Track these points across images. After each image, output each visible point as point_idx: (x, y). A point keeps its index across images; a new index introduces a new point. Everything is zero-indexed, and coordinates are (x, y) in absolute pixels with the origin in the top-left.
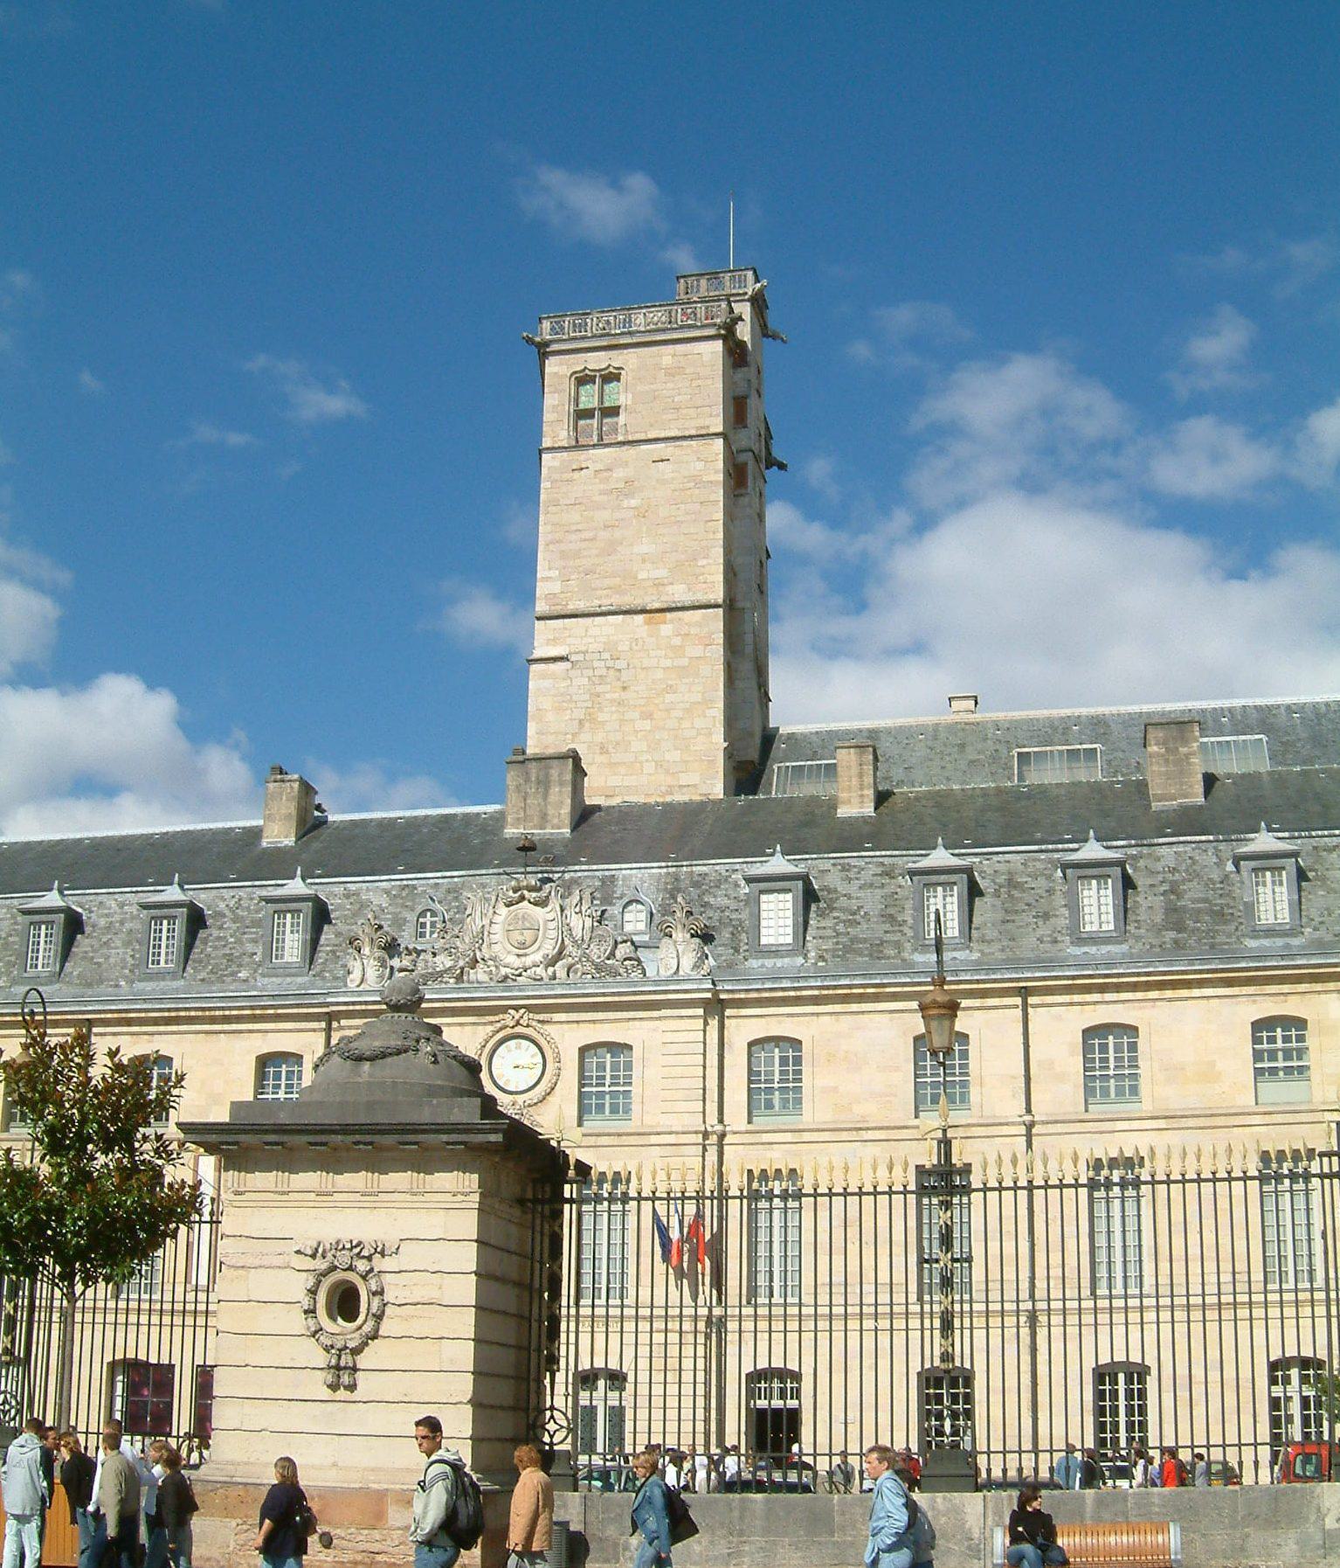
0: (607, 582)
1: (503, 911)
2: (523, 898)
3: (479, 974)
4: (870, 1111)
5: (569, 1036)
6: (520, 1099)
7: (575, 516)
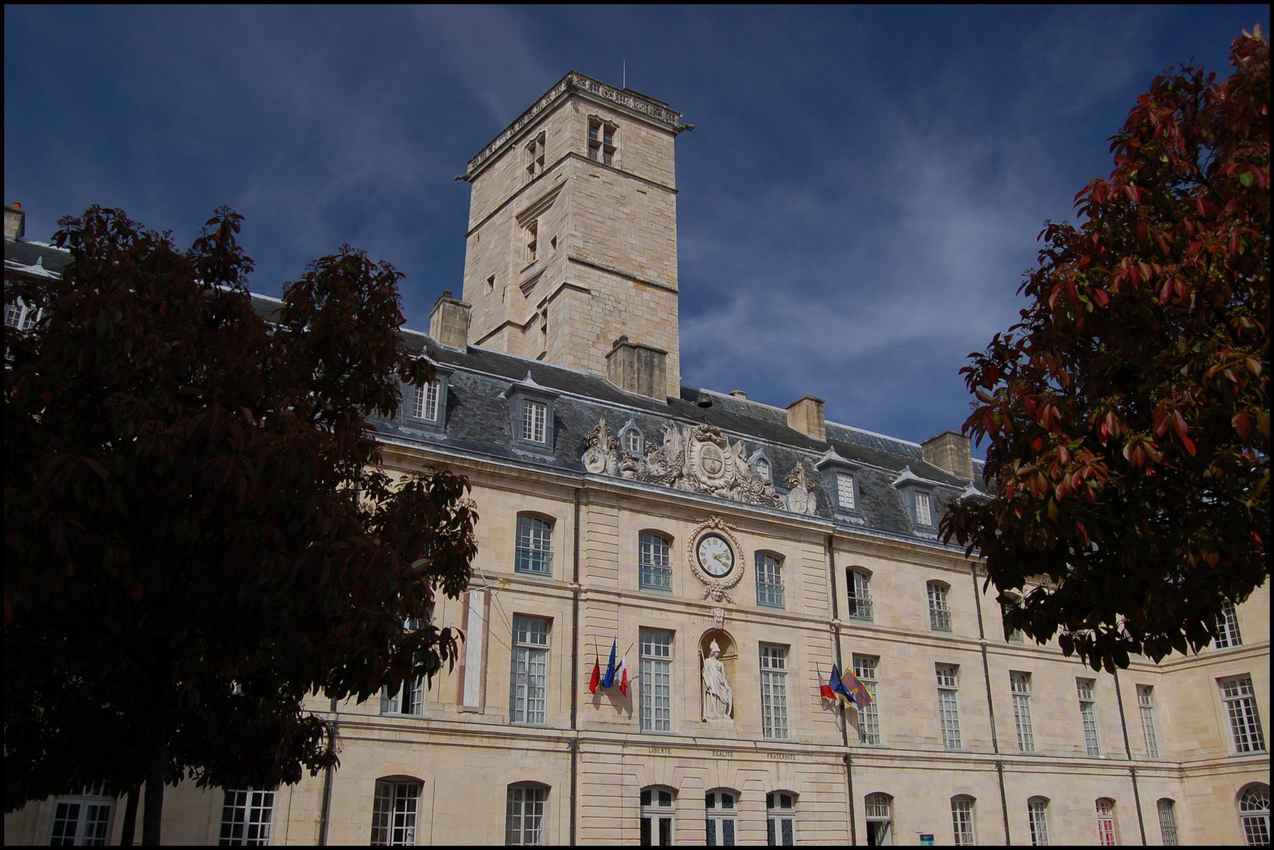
0: (612, 253)
1: (698, 445)
2: (710, 439)
3: (685, 484)
4: (908, 623)
5: (750, 543)
6: (722, 581)
7: (590, 204)
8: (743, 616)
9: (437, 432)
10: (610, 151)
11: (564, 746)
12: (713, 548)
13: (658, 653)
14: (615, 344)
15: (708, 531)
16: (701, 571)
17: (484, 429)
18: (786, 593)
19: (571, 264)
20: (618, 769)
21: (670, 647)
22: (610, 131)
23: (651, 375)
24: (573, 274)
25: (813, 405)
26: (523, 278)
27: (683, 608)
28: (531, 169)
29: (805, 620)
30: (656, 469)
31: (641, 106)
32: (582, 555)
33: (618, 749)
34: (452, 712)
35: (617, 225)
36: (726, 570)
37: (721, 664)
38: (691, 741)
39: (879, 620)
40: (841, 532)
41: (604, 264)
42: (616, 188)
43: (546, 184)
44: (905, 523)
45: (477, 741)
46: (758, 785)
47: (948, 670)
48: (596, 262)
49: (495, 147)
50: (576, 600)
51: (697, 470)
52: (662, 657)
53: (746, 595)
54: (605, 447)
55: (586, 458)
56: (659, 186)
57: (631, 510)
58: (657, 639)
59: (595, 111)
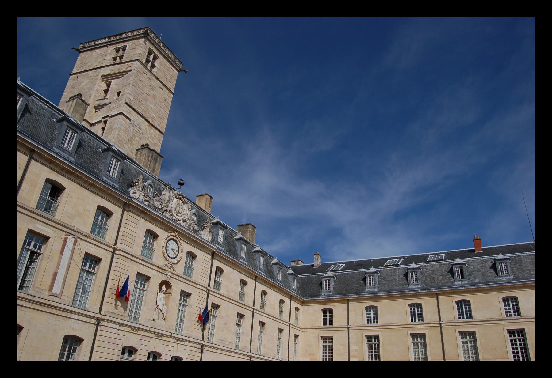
1: (176, 200)
2: (180, 199)
5: (187, 247)
6: (173, 260)
7: (140, 84)
8: (177, 277)
9: (70, 156)
10: (153, 66)
11: (94, 321)
12: (172, 245)
13: (141, 286)
14: (142, 146)
16: (165, 254)
17: (91, 162)
18: (194, 272)
19: (126, 106)
20: (115, 336)
21: (147, 284)
22: (155, 58)
23: (155, 164)
24: (126, 110)
25: (209, 198)
26: (97, 103)
27: (155, 268)
28: (115, 59)
29: (199, 285)
30: (157, 204)
31: (169, 54)
32: (120, 234)
33: (117, 326)
34: (45, 294)
35: (148, 97)
36: (175, 256)
37: (165, 296)
38: (147, 328)
39: (222, 291)
40: (218, 252)
41: (139, 111)
42: (152, 82)
43: (122, 68)
44: (237, 254)
45: (54, 311)
46: (169, 353)
47: (241, 316)
48: (136, 109)
49: (97, 43)
50: (113, 253)
51: (173, 210)
52: (142, 288)
53: (180, 269)
54: (140, 188)
55: (131, 190)
56: (168, 89)
57: (145, 219)
58: (144, 278)
59: (152, 47)
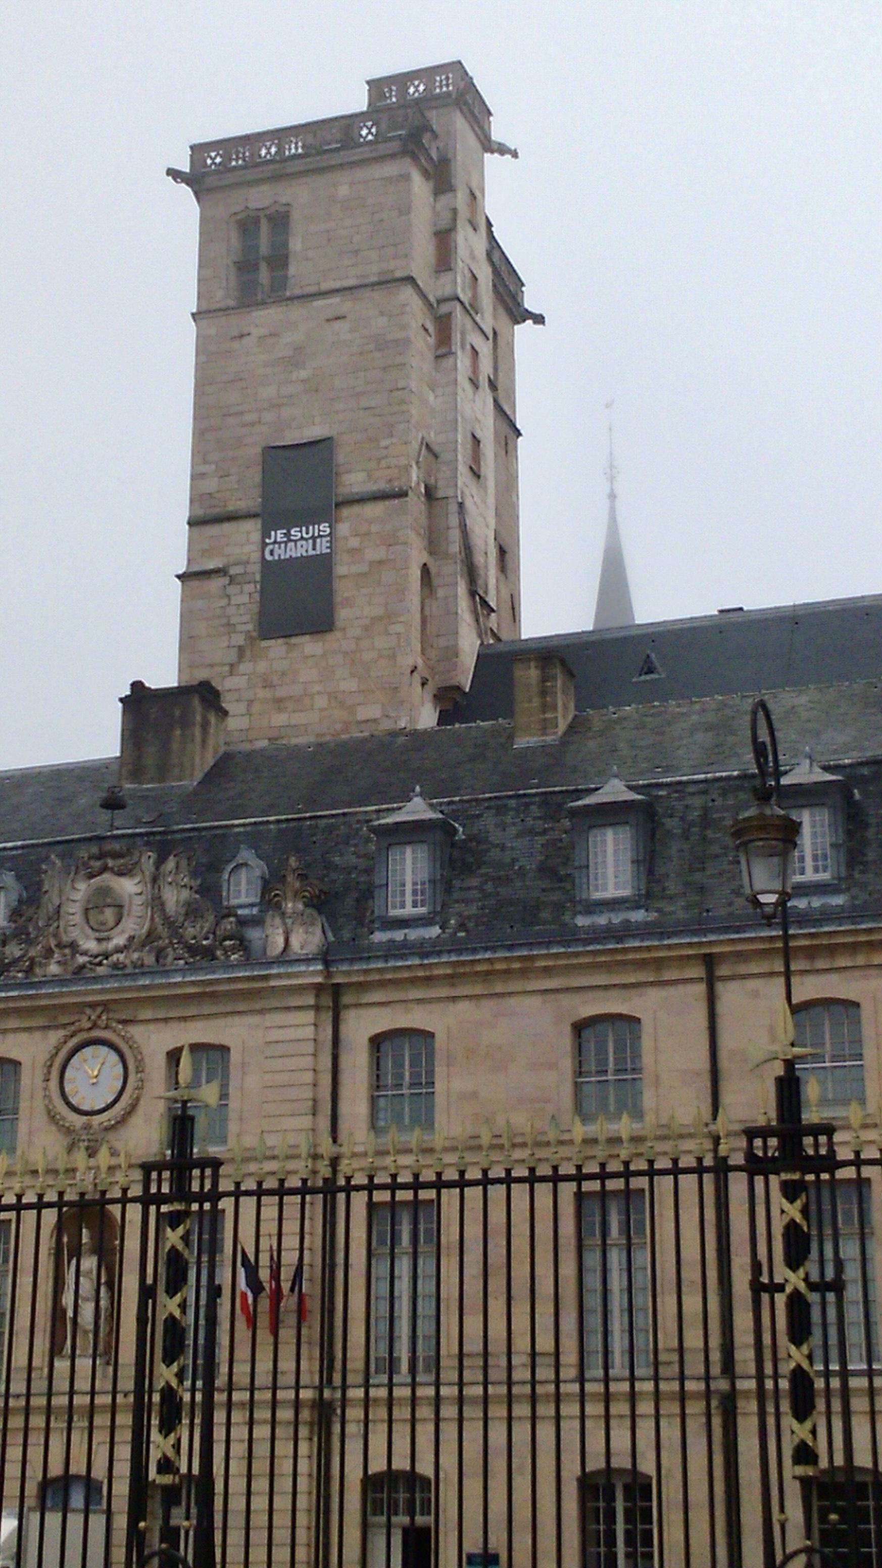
6: (96, 1120)
15: (83, 1036)
22: (280, 221)
